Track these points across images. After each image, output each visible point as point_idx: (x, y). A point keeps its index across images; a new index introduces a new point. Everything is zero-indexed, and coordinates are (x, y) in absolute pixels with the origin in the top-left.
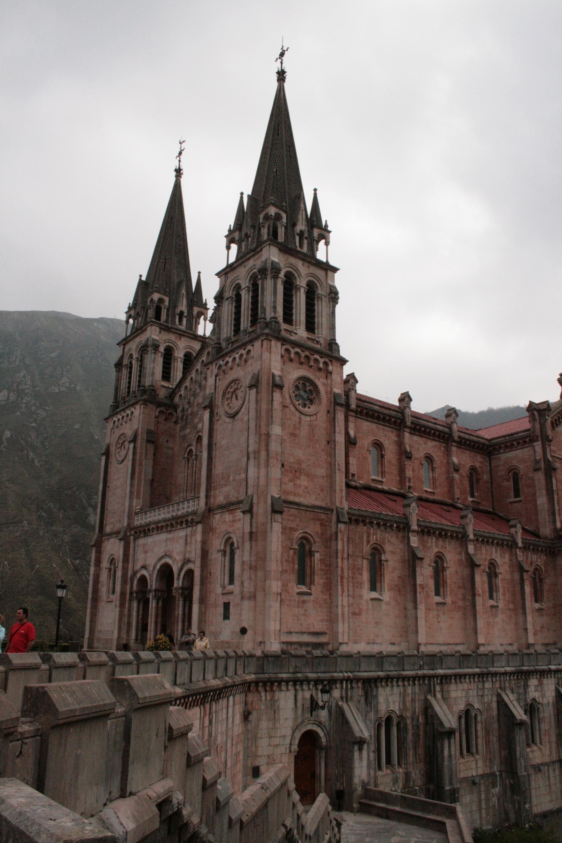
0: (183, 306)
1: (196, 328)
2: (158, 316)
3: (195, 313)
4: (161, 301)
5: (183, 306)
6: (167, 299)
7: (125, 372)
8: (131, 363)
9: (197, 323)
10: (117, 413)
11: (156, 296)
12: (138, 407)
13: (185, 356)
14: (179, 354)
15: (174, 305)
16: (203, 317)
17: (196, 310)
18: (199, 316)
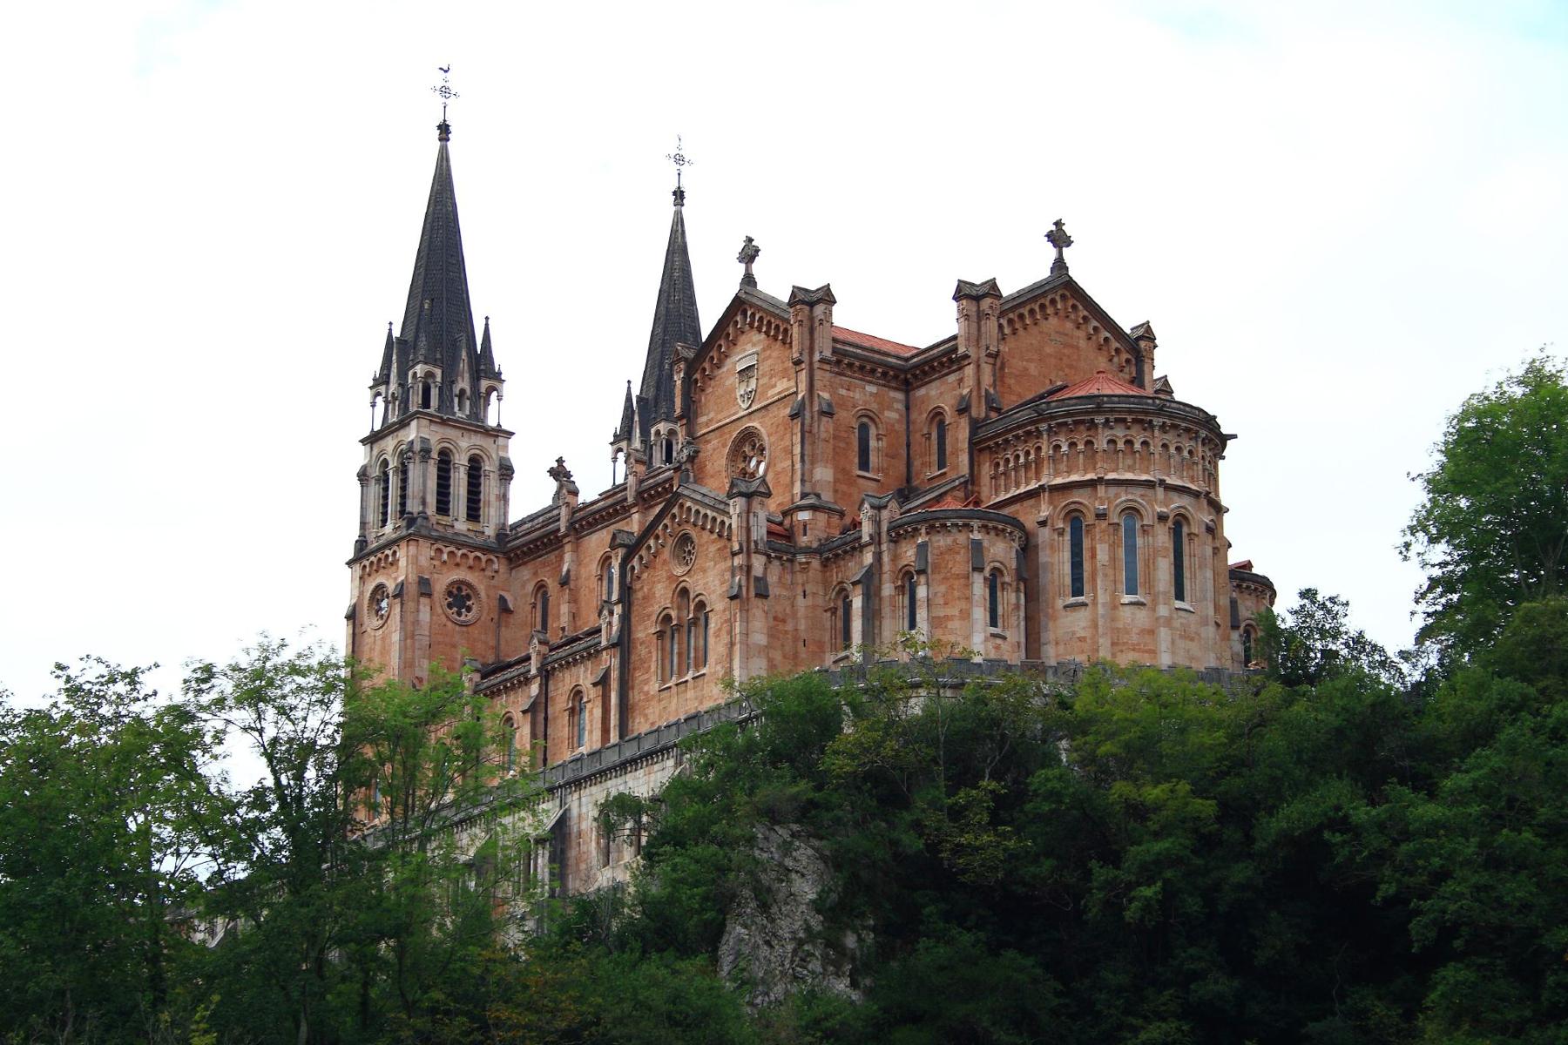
0: (464, 384)
1: (485, 416)
2: (426, 403)
3: (483, 390)
4: (429, 375)
5: (464, 384)
6: (438, 372)
7: (375, 490)
8: (386, 474)
9: (487, 403)
10: (369, 554)
11: (420, 369)
12: (403, 544)
13: (470, 460)
14: (461, 460)
15: (449, 381)
16: (494, 394)
17: (484, 384)
18: (488, 394)
